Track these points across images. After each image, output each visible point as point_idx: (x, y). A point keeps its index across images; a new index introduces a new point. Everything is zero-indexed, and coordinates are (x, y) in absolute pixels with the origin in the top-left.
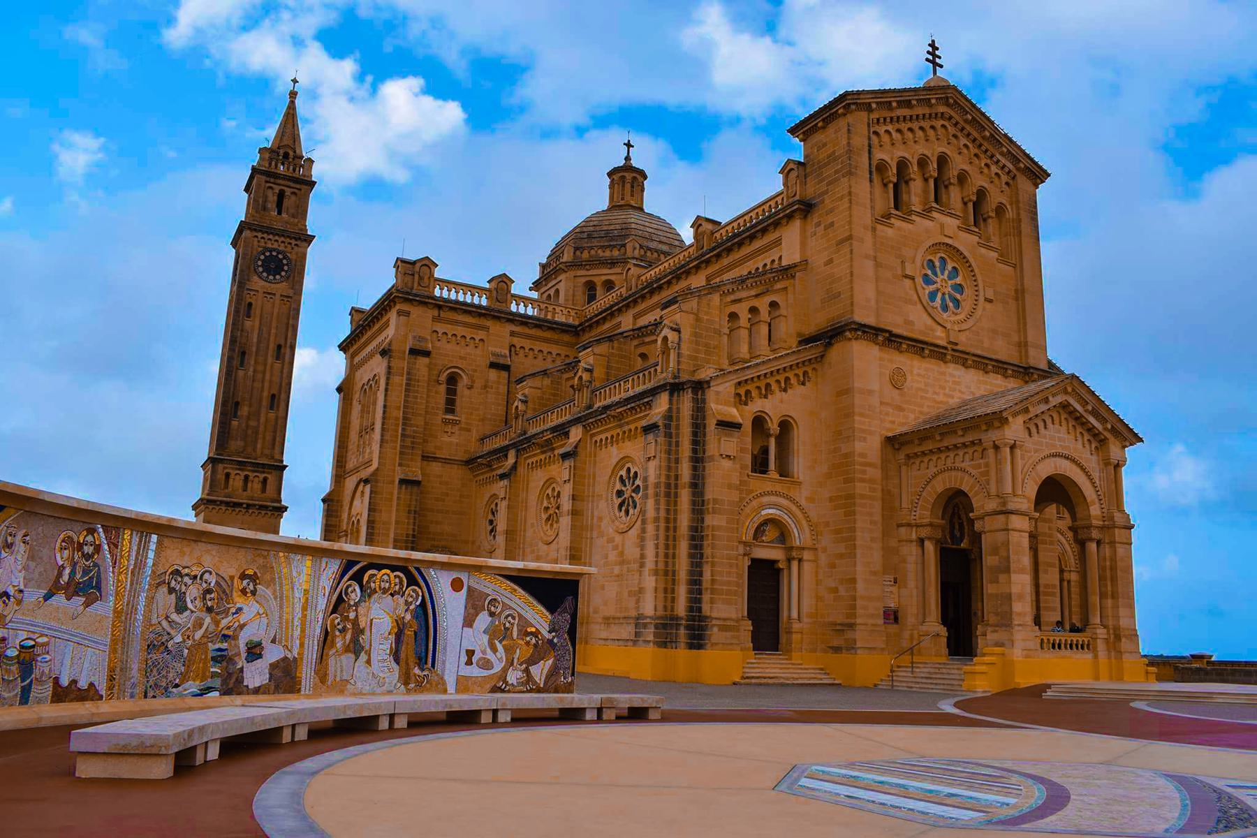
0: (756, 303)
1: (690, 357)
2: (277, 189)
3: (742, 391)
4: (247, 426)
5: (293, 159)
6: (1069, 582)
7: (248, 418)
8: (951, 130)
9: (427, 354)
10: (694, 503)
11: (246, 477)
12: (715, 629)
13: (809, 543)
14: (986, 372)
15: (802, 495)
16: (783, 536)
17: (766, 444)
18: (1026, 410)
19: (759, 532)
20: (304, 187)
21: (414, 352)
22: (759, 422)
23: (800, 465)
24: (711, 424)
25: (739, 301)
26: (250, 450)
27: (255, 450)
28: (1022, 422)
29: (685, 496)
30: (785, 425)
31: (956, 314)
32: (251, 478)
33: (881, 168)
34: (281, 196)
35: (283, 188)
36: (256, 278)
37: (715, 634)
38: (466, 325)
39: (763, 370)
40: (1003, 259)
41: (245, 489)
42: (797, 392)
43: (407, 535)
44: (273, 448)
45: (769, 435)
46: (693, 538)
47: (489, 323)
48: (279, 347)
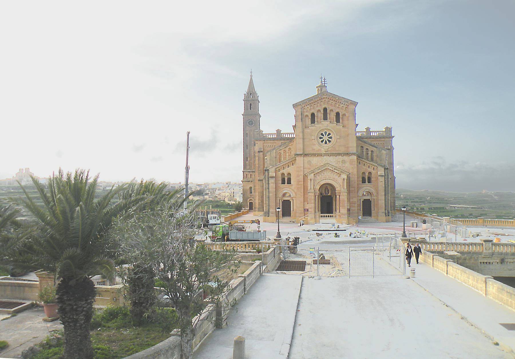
0: (285, 149)
1: (269, 164)
3: (278, 169)
4: (250, 163)
5: (253, 94)
6: (374, 199)
7: (250, 160)
8: (327, 100)
9: (262, 152)
10: (268, 191)
11: (251, 174)
12: (271, 213)
13: (295, 196)
14: (336, 156)
15: (293, 187)
16: (290, 196)
17: (289, 177)
18: (314, 172)
19: (284, 195)
20: (255, 101)
21: (259, 152)
22: (283, 174)
25: (281, 150)
26: (251, 168)
27: (252, 168)
28: (313, 174)
30: (289, 174)
31: (329, 144)
32: (252, 175)
33: (307, 116)
34: (251, 105)
35: (251, 103)
37: (270, 214)
38: (271, 143)
39: (287, 162)
41: (251, 177)
42: (291, 167)
43: (261, 191)
45: (285, 177)
46: (268, 198)
47: (276, 141)
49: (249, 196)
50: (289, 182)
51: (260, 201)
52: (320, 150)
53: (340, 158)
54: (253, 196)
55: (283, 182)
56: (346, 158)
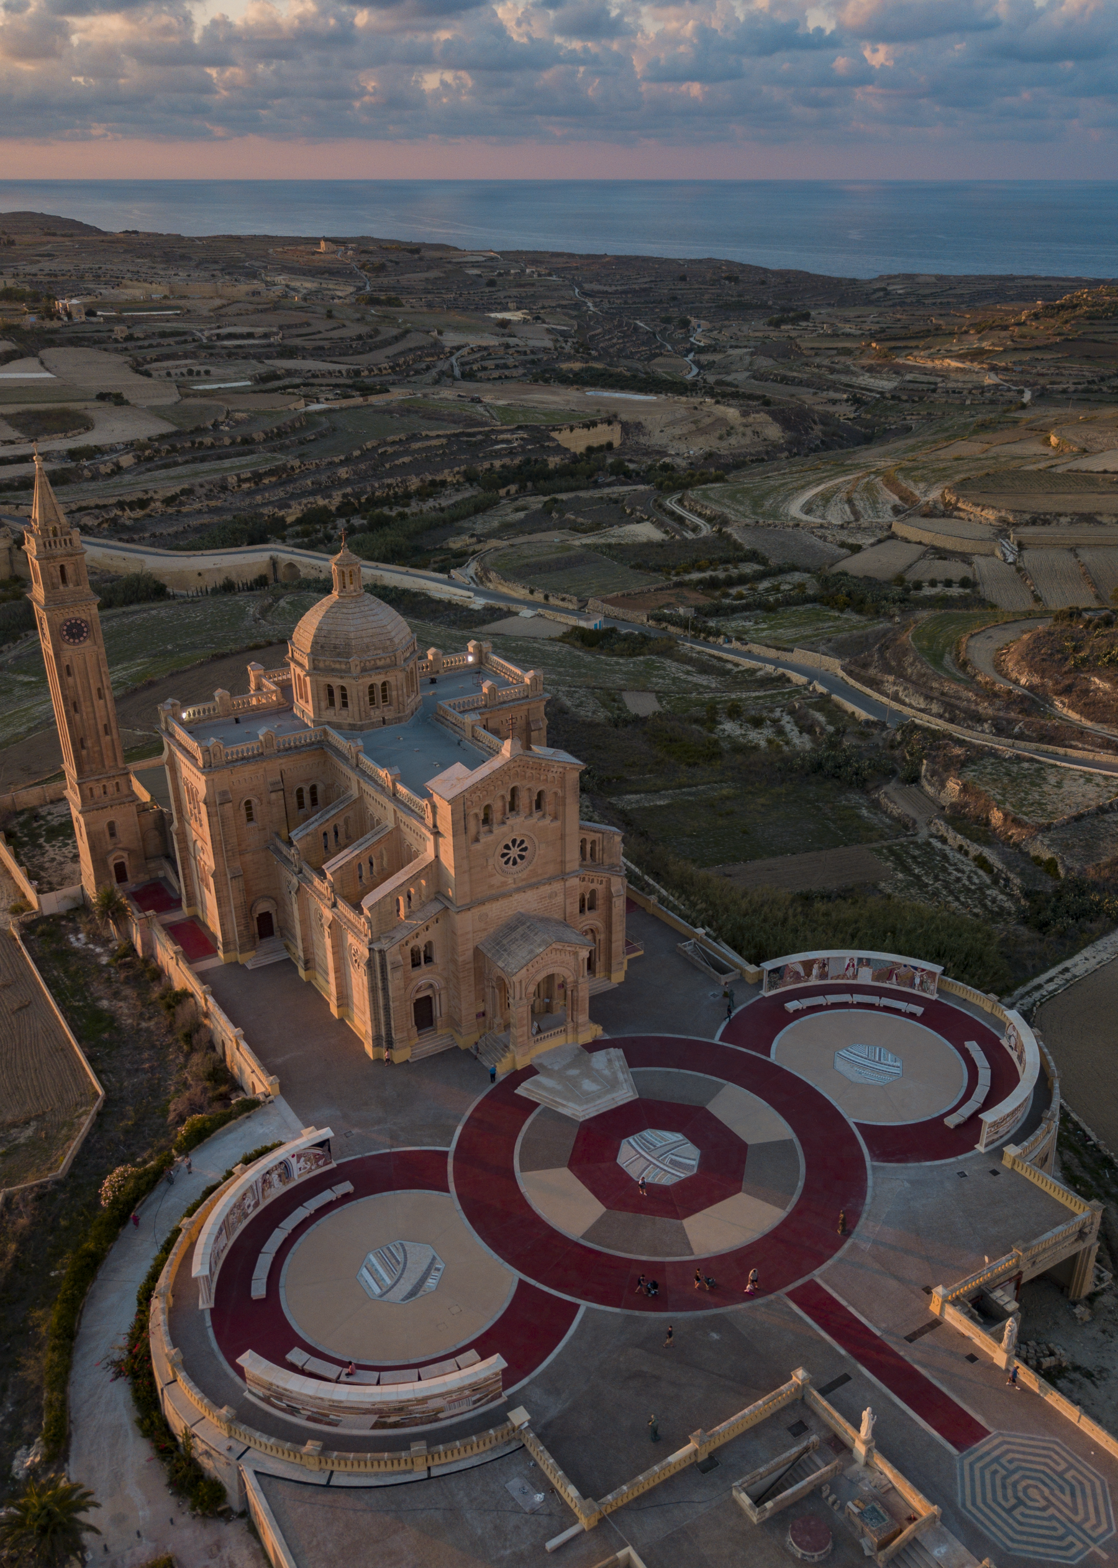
2: (58, 566)
11: (104, 786)
20: (78, 557)
23: (437, 957)
24: (389, 968)
29: (380, 994)
34: (62, 567)
36: (66, 646)
40: (555, 818)
44: (116, 760)
48: (99, 690)
49: (110, 848)
50: (428, 959)
51: (242, 928)
52: (504, 884)
53: (546, 890)
54: (120, 846)
55: (416, 964)
56: (557, 886)
